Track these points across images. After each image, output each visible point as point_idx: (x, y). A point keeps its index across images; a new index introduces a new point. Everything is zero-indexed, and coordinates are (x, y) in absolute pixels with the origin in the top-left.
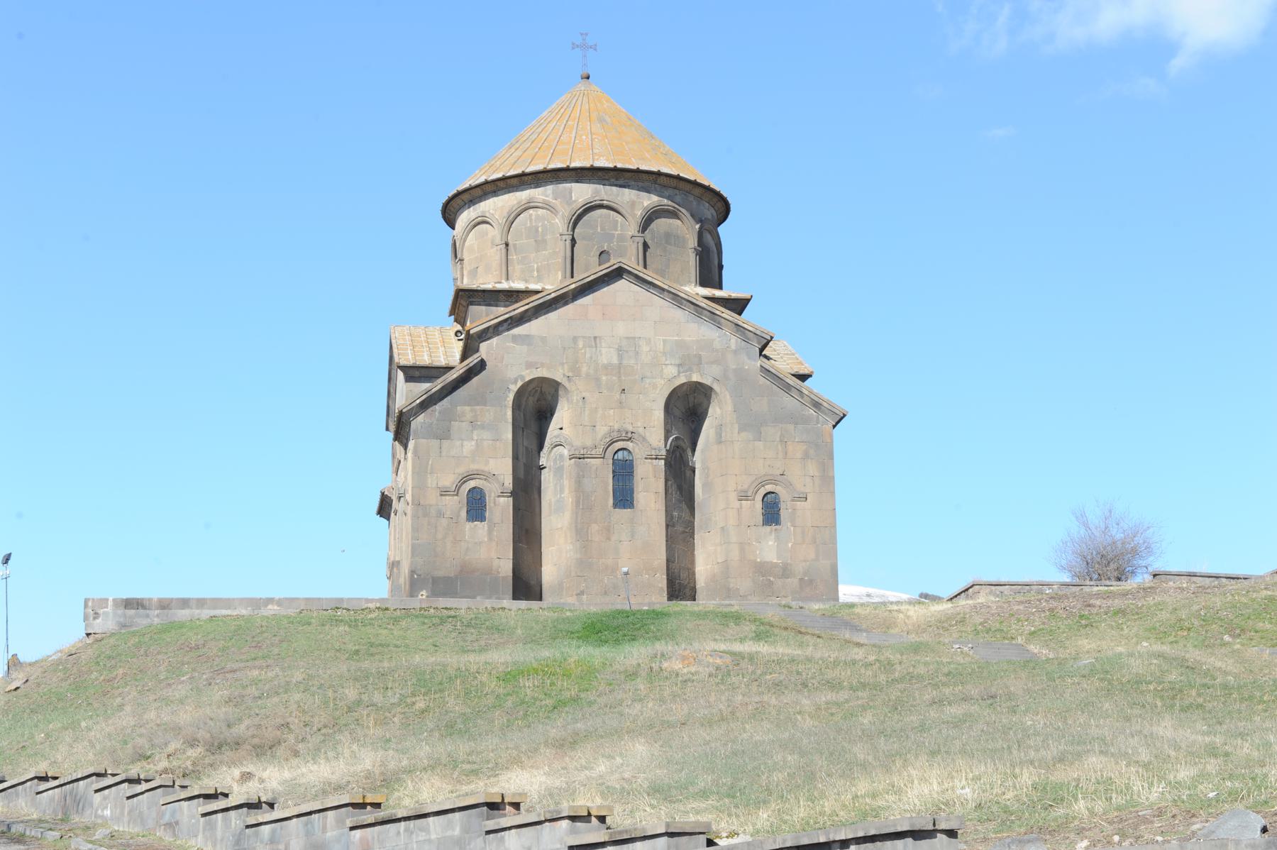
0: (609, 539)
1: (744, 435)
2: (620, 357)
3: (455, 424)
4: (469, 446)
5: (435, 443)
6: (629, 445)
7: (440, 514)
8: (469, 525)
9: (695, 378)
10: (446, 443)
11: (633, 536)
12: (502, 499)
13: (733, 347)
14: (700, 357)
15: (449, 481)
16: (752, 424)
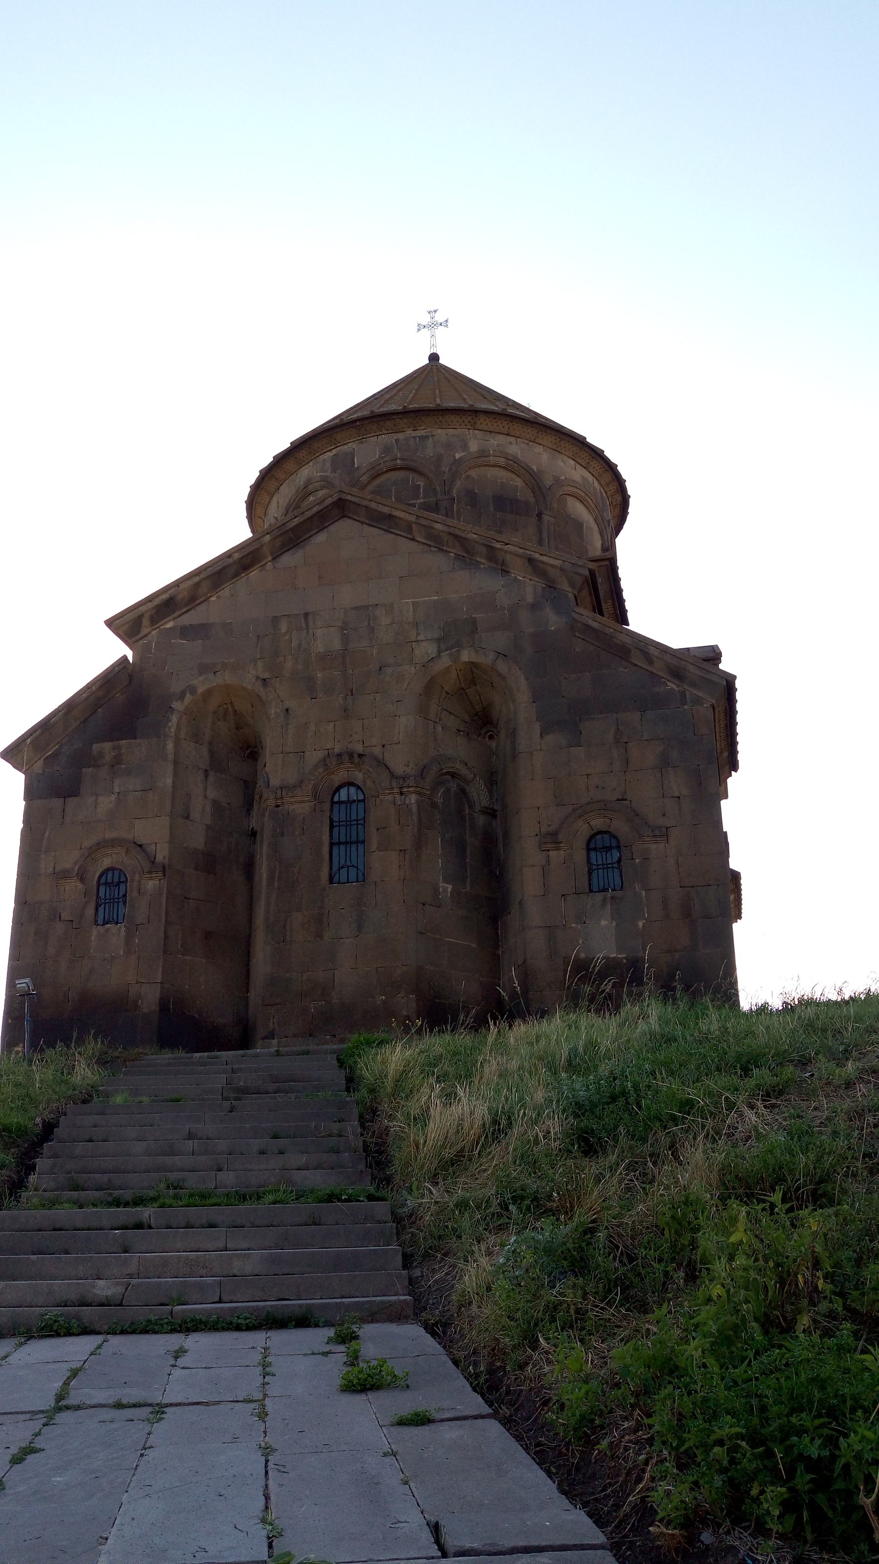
0: (320, 936)
1: (549, 738)
2: (345, 639)
3: (88, 771)
4: (106, 803)
5: (56, 803)
6: (359, 777)
7: (55, 916)
8: (95, 932)
9: (466, 656)
10: (72, 802)
11: (360, 928)
12: (151, 885)
13: (530, 599)
14: (474, 622)
15: (69, 860)
16: (566, 720)
